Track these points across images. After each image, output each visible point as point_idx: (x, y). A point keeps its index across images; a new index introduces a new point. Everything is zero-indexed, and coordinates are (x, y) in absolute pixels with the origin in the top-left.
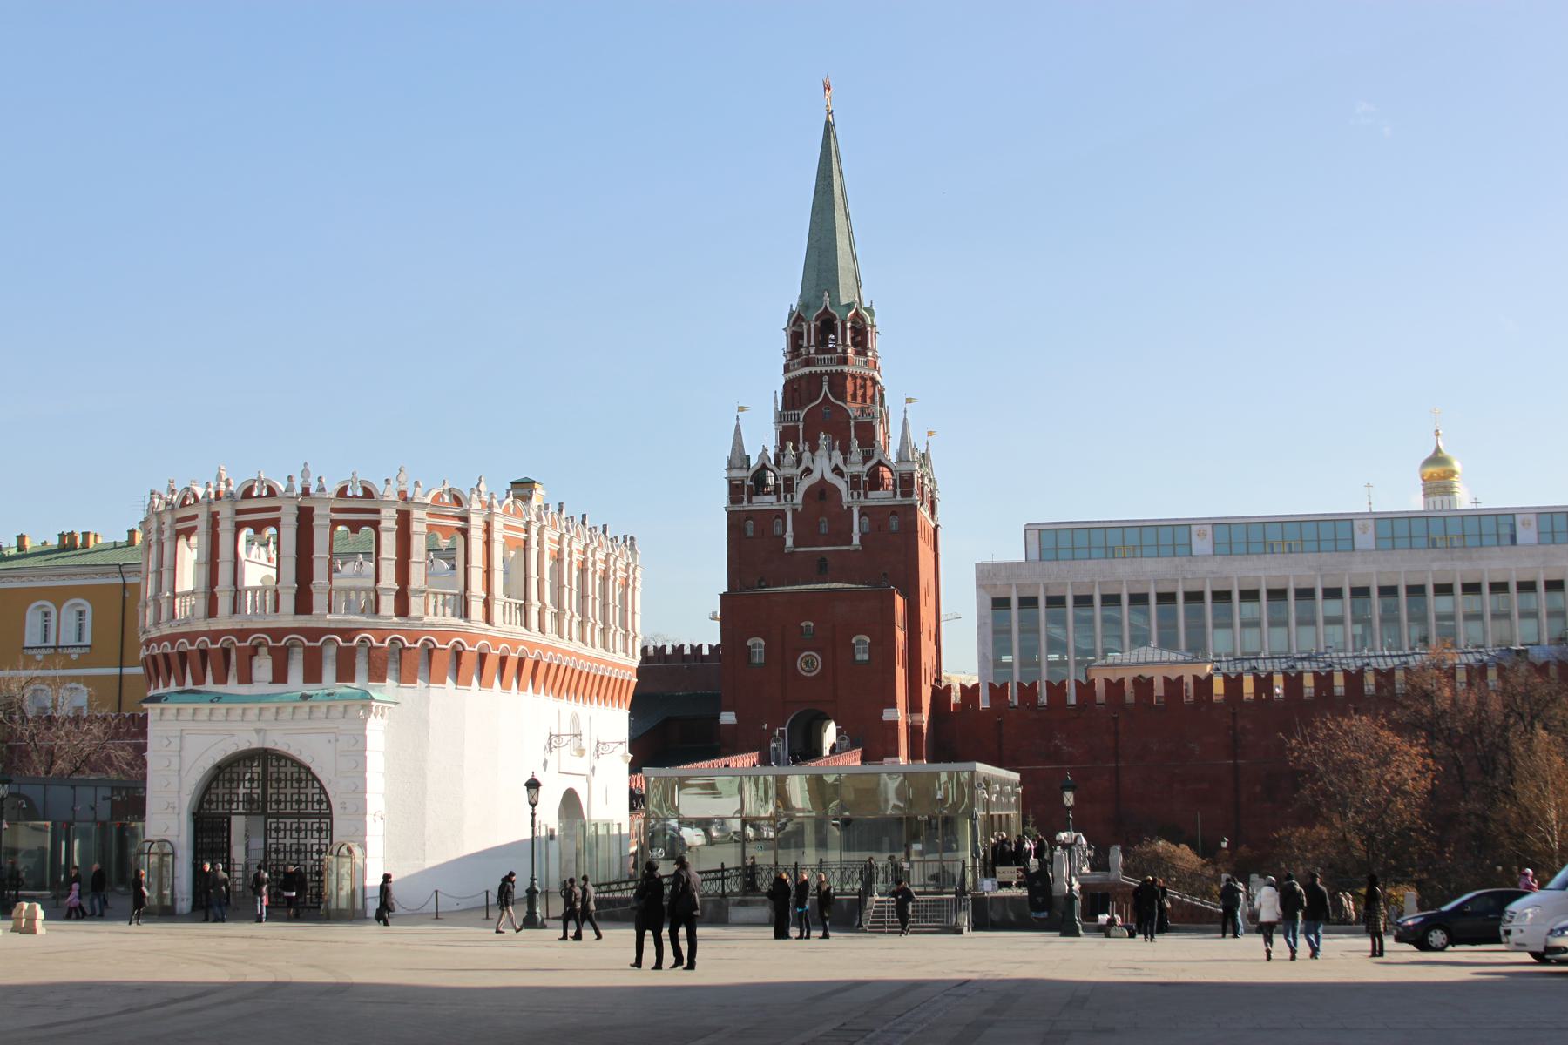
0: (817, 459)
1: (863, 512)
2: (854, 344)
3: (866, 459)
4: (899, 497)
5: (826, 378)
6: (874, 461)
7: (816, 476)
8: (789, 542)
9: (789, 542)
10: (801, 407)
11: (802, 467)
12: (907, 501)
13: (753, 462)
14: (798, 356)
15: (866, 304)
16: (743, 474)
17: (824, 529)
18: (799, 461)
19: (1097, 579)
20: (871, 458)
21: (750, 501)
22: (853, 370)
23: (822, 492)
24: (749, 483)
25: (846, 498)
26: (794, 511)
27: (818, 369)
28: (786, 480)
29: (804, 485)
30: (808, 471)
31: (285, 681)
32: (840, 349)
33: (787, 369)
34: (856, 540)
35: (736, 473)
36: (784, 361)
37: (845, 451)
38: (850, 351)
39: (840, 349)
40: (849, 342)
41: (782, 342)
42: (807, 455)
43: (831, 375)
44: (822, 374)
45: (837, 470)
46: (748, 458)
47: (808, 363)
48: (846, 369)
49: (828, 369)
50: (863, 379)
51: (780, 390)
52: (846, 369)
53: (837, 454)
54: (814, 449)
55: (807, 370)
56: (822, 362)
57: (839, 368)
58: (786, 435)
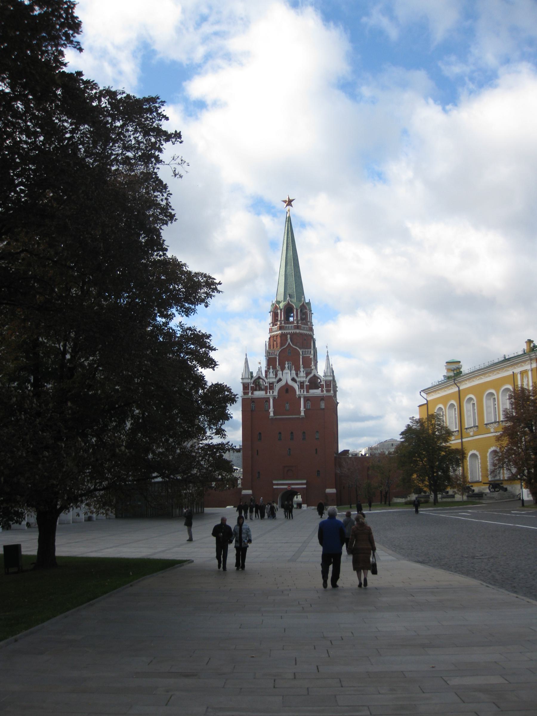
1: (307, 399)
2: (302, 319)
3: (307, 374)
7: (283, 383)
8: (272, 414)
9: (272, 414)
11: (278, 378)
13: (255, 375)
14: (276, 325)
15: (307, 301)
16: (249, 381)
17: (287, 406)
18: (276, 375)
20: (311, 373)
23: (287, 389)
25: (298, 393)
26: (274, 399)
27: (286, 332)
28: (270, 384)
29: (278, 387)
30: (280, 380)
31: (6, 548)
32: (295, 322)
33: (271, 331)
34: (302, 414)
35: (246, 381)
36: (269, 327)
37: (297, 370)
38: (300, 322)
40: (299, 318)
42: (280, 373)
44: (287, 334)
45: (293, 380)
46: (252, 373)
47: (281, 328)
48: (298, 331)
49: (290, 331)
50: (306, 335)
51: (268, 340)
52: (298, 331)
53: (294, 372)
54: (283, 369)
56: (287, 328)
58: (270, 362)
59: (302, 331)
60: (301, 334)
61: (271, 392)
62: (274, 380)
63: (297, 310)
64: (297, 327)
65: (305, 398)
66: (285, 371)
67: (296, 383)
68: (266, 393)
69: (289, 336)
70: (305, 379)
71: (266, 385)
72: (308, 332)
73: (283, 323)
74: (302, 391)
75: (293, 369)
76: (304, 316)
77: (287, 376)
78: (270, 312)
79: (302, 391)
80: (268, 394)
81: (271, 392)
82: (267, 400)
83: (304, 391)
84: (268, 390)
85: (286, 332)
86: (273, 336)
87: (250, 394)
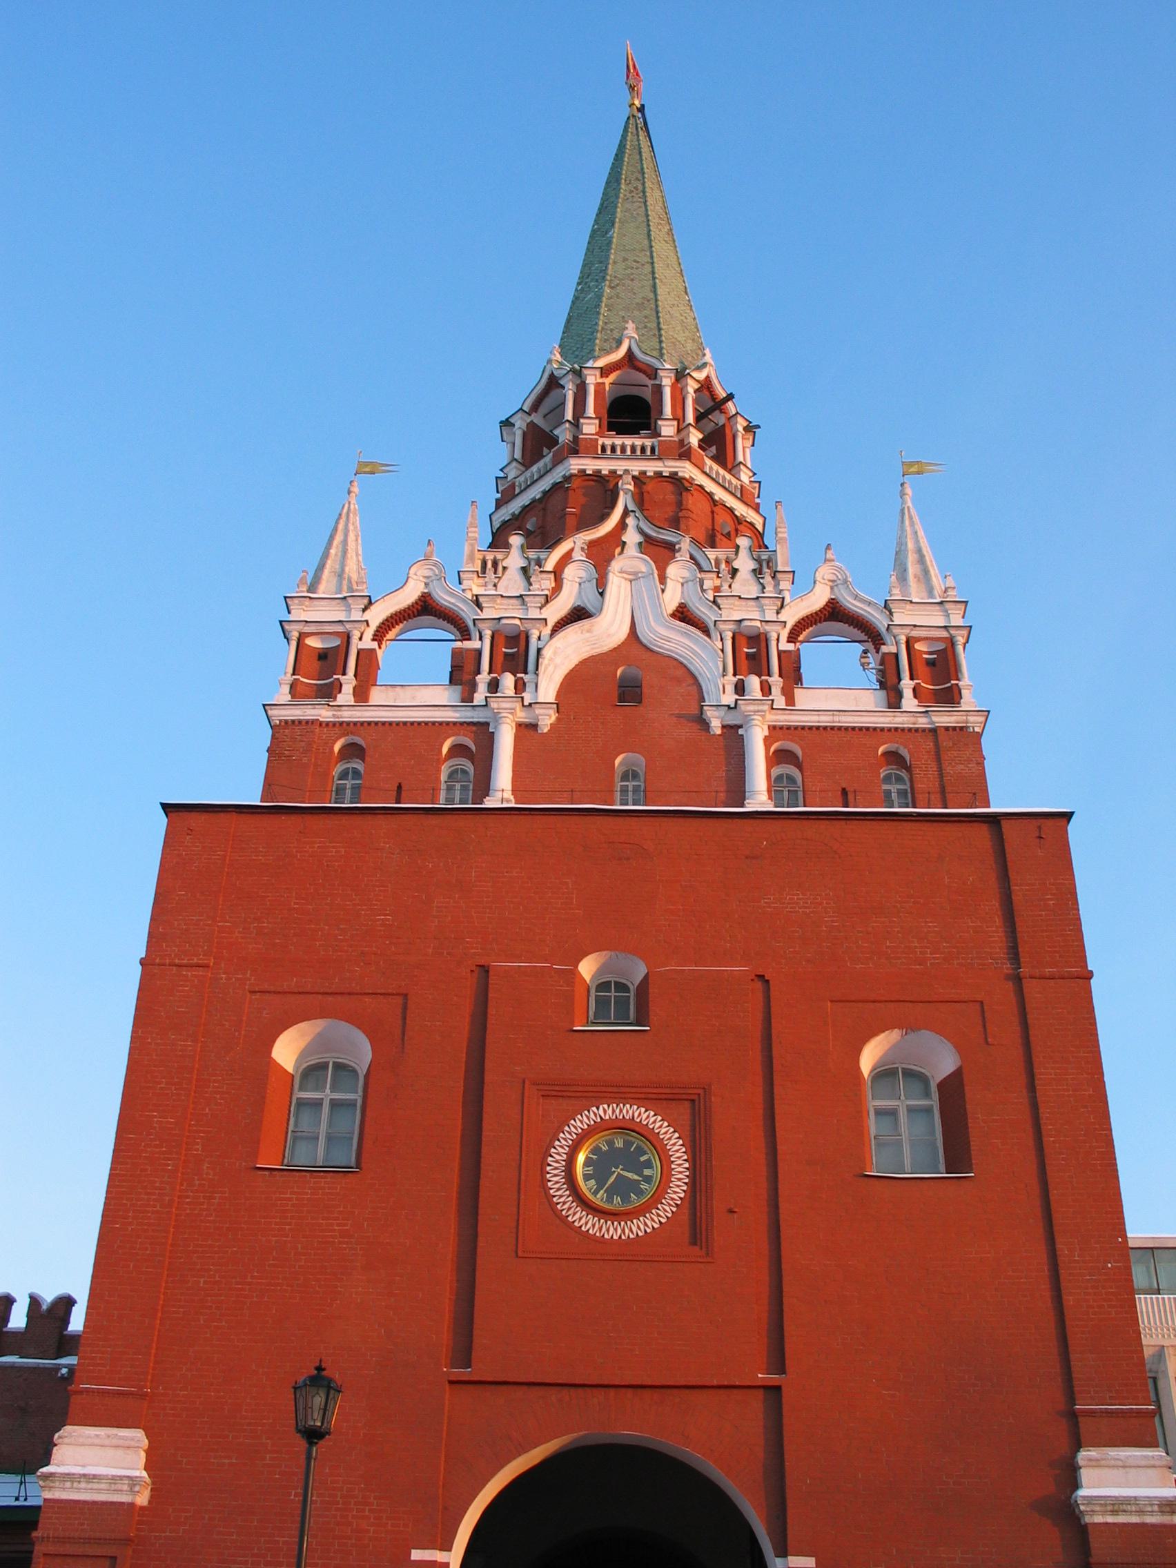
0: (616, 584)
4: (909, 702)
5: (627, 485)
6: (817, 600)
12: (944, 718)
21: (361, 694)
22: (701, 479)
24: (368, 643)
26: (526, 730)
27: (605, 466)
30: (578, 614)
39: (668, 429)
40: (690, 418)
41: (497, 455)
43: (639, 480)
45: (683, 614)
49: (636, 467)
52: (686, 470)
57: (667, 467)
59: (710, 486)
61: (508, 681)
63: (680, 375)
64: (684, 453)
65: (776, 731)
66: (616, 566)
67: (706, 632)
68: (468, 698)
69: (627, 485)
71: (474, 644)
72: (740, 509)
73: (590, 428)
77: (629, 602)
78: (507, 423)
79: (754, 682)
84: (483, 678)
86: (525, 509)
87: (346, 696)
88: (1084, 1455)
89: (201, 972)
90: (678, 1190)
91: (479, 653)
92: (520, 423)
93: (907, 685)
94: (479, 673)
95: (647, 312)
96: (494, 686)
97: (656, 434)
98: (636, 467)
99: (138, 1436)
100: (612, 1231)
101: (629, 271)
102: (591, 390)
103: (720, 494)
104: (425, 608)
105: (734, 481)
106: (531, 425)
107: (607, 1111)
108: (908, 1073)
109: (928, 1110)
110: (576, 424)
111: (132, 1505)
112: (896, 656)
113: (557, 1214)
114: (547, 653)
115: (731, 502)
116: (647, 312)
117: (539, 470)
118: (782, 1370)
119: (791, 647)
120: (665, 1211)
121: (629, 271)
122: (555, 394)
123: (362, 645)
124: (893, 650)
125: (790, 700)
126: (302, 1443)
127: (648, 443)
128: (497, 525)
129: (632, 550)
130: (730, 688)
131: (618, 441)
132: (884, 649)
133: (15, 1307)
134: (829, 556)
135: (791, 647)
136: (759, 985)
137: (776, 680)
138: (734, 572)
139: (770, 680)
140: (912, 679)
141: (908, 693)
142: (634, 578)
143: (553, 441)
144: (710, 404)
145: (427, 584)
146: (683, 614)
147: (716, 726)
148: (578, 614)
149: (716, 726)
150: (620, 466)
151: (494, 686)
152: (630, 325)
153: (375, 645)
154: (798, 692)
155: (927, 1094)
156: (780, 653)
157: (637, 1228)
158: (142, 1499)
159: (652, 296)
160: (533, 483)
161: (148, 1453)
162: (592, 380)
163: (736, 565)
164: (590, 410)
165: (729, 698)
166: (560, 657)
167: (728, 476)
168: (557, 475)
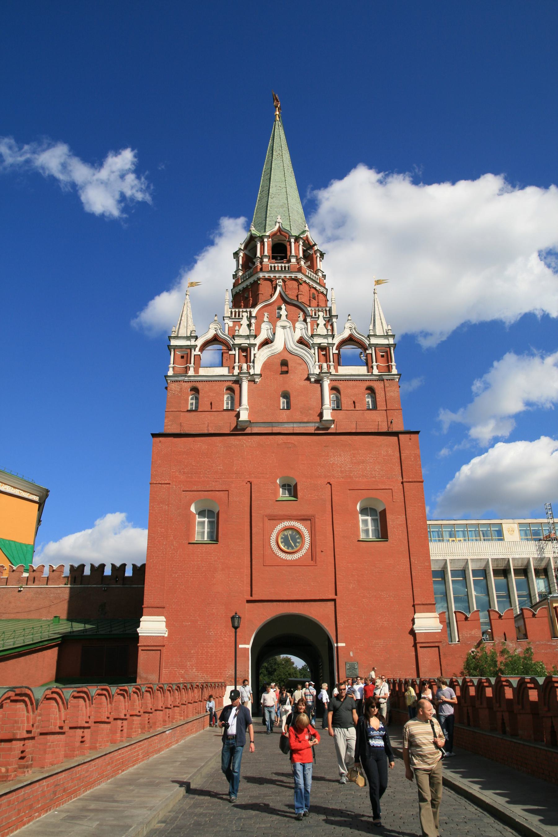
0: (279, 331)
4: (376, 371)
6: (346, 334)
10: (254, 306)
19: (448, 558)
21: (196, 371)
22: (305, 279)
23: (283, 365)
24: (197, 352)
27: (272, 275)
30: (267, 342)
36: (234, 281)
38: (302, 263)
39: (293, 260)
40: (301, 255)
45: (301, 341)
48: (300, 276)
49: (283, 276)
50: (315, 289)
52: (300, 276)
55: (261, 275)
59: (308, 281)
60: (305, 282)
61: (245, 366)
62: (252, 341)
64: (300, 270)
66: (279, 324)
70: (330, 340)
72: (318, 287)
73: (266, 260)
74: (325, 365)
75: (301, 318)
76: (309, 263)
79: (325, 365)
80: (236, 371)
81: (245, 366)
82: (234, 387)
83: (329, 367)
85: (272, 275)
87: (191, 372)
88: (417, 615)
89: (168, 485)
90: (307, 545)
91: (235, 355)
92: (241, 254)
93: (374, 363)
94: (235, 363)
95: (285, 209)
96: (240, 368)
97: (289, 261)
98: (283, 276)
99: (163, 618)
100: (289, 557)
101: (278, 191)
102: (266, 244)
103: (311, 283)
104: (215, 340)
105: (317, 277)
106: (245, 254)
107: (287, 524)
108: (371, 509)
109: (377, 520)
110: (262, 259)
111: (163, 636)
112: (371, 354)
113: (274, 553)
114: (256, 356)
115: (315, 285)
116: (285, 209)
117: (248, 274)
118: (336, 595)
119: (337, 352)
120: (303, 551)
121: (278, 191)
122: (253, 242)
123: (195, 353)
124: (371, 352)
125: (337, 371)
126: (234, 630)
127: (287, 265)
128: (234, 293)
129: (284, 317)
130: (317, 367)
131: (276, 265)
132: (367, 352)
133: (85, 568)
134: (349, 318)
135: (337, 352)
136: (328, 484)
137: (332, 363)
138: (318, 325)
139: (330, 364)
140: (376, 362)
141: (375, 367)
142: (284, 327)
143: (254, 263)
144: (308, 246)
145: (216, 331)
146: (301, 341)
147: (313, 380)
148: (267, 342)
149: (313, 380)
150: (277, 275)
151: (240, 368)
152: (279, 217)
153: (199, 353)
154: (339, 367)
155: (377, 516)
156: (333, 354)
157: (296, 556)
158: (166, 635)
159: (286, 202)
160: (247, 279)
161: (167, 622)
162: (266, 240)
163: (318, 322)
164: (266, 253)
165: (317, 371)
166: (261, 357)
167: (314, 275)
168: (254, 278)
